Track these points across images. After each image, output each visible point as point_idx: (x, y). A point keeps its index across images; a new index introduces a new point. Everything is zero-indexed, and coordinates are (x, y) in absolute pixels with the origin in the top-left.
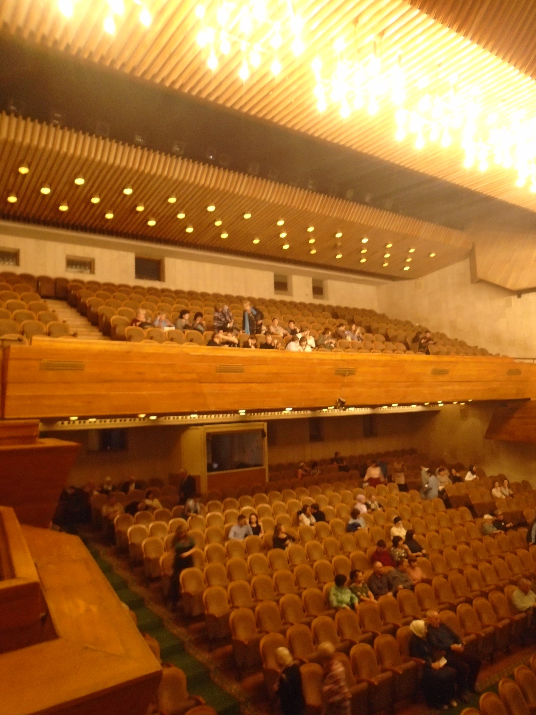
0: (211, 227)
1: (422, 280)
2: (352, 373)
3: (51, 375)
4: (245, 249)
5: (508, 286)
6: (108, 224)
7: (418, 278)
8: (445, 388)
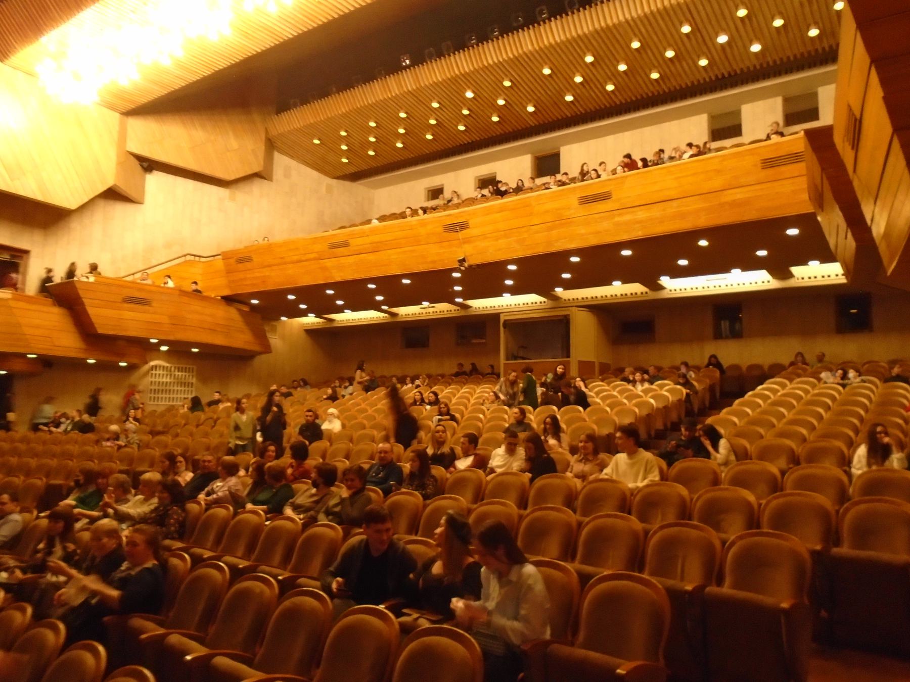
8: (617, 219)
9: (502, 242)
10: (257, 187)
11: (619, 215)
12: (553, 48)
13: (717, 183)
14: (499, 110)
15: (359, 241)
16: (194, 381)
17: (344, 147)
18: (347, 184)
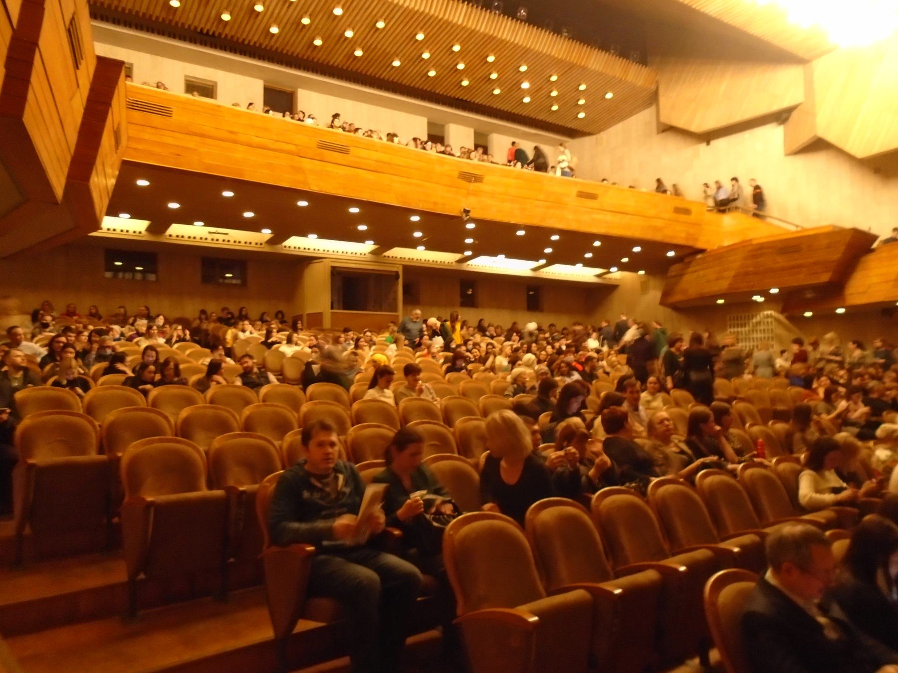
0: (342, 40)
1: (603, 135)
3: (137, 115)
4: (385, 75)
5: (694, 128)
6: (228, 29)
7: (599, 131)
13: (652, 212)
15: (363, 153)
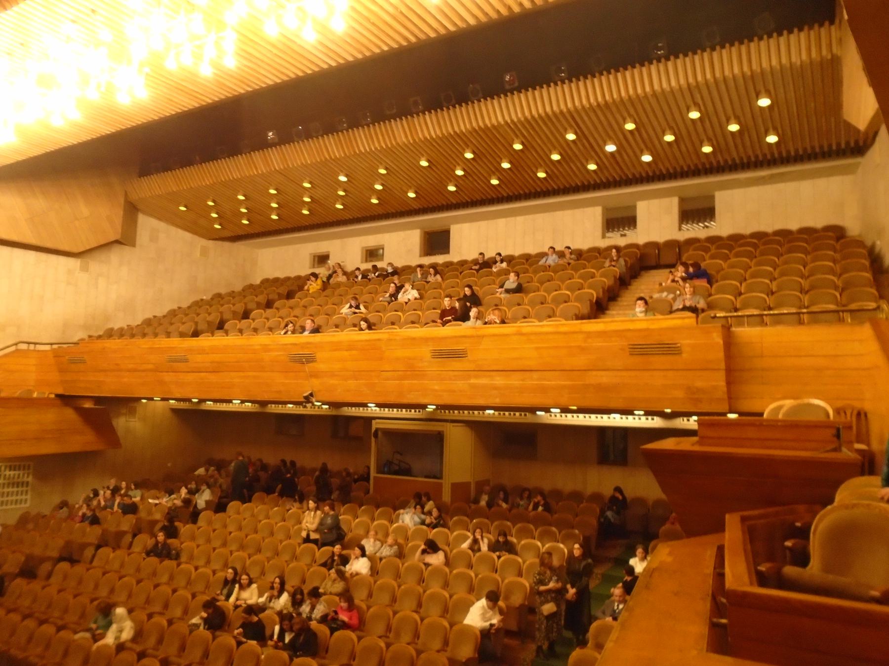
2: (310, 359)
8: (473, 381)
9: (352, 383)
10: (115, 255)
11: (476, 377)
12: (429, 143)
13: (580, 361)
14: (379, 194)
15: (199, 358)
16: (30, 479)
17: (214, 215)
18: (227, 244)
